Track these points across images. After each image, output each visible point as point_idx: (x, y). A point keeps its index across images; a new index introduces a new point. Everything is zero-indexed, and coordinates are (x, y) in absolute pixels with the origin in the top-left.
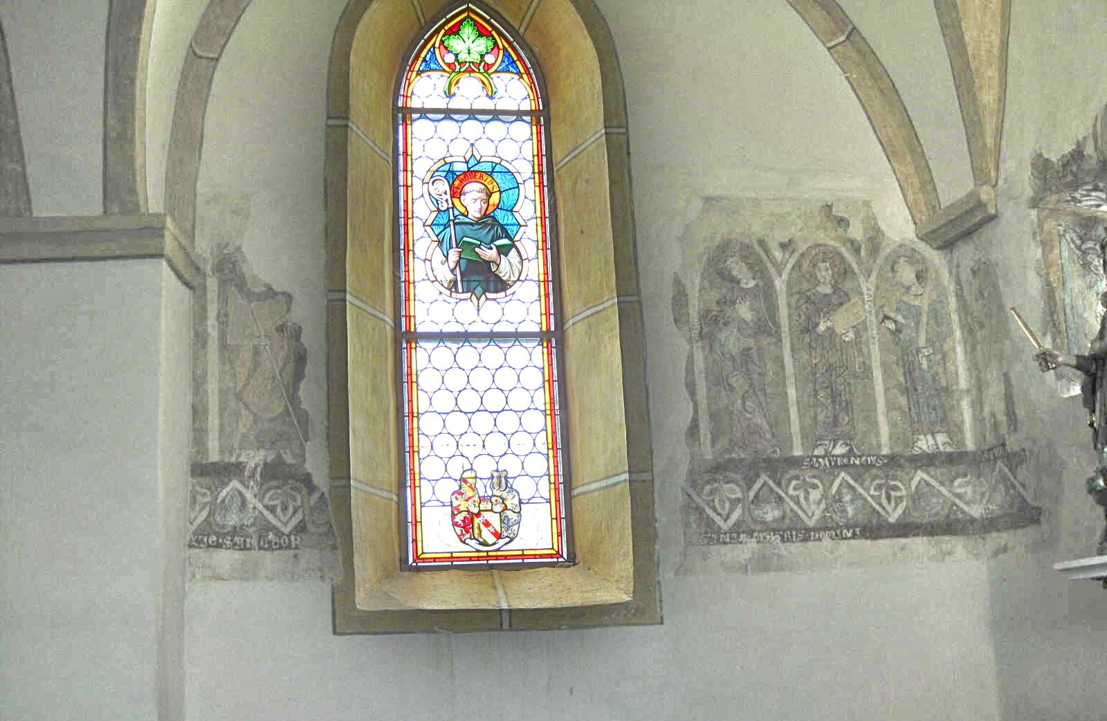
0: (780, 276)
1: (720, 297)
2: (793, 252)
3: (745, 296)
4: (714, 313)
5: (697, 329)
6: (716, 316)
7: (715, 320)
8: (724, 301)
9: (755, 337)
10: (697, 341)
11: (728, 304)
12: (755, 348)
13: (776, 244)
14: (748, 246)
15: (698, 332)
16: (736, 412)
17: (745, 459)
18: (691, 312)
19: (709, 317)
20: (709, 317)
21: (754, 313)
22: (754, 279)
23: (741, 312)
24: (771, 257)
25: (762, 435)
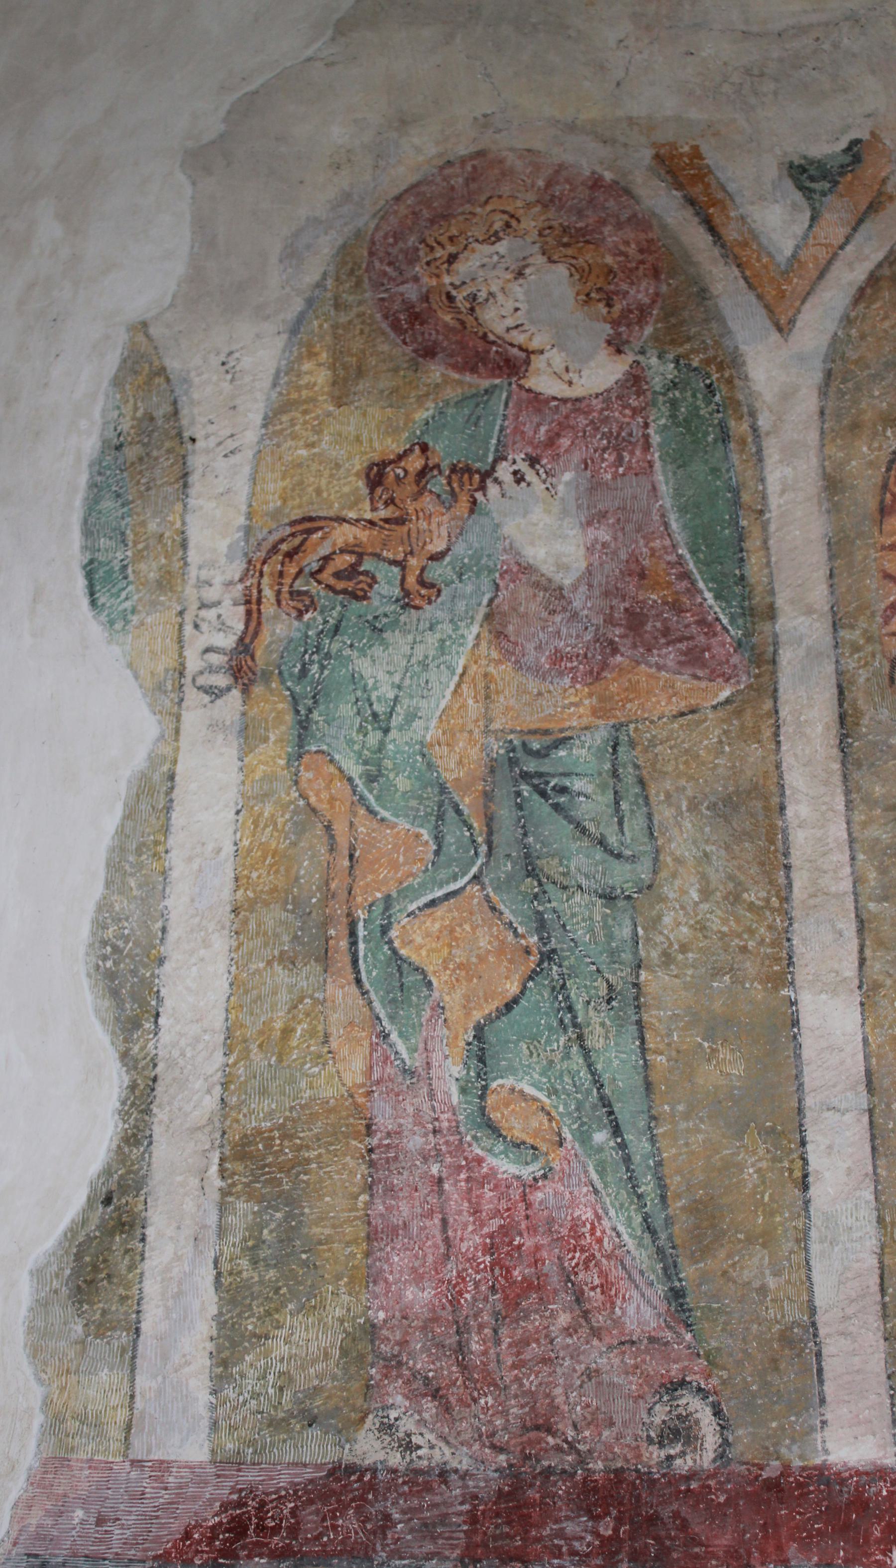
0: (783, 328)
1: (394, 446)
2: (874, 207)
3: (551, 442)
4: (343, 534)
5: (223, 627)
6: (358, 552)
7: (352, 571)
8: (415, 463)
9: (595, 676)
10: (215, 693)
11: (438, 484)
12: (601, 735)
13: (771, 170)
14: (596, 183)
15: (228, 641)
16: (415, 1142)
17: (444, 1475)
18: (196, 535)
19: (311, 561)
20: (311, 561)
21: (604, 535)
22: (617, 346)
23: (510, 528)
24: (731, 234)
25: (596, 1297)
